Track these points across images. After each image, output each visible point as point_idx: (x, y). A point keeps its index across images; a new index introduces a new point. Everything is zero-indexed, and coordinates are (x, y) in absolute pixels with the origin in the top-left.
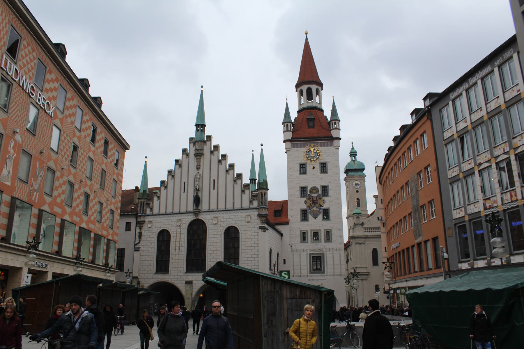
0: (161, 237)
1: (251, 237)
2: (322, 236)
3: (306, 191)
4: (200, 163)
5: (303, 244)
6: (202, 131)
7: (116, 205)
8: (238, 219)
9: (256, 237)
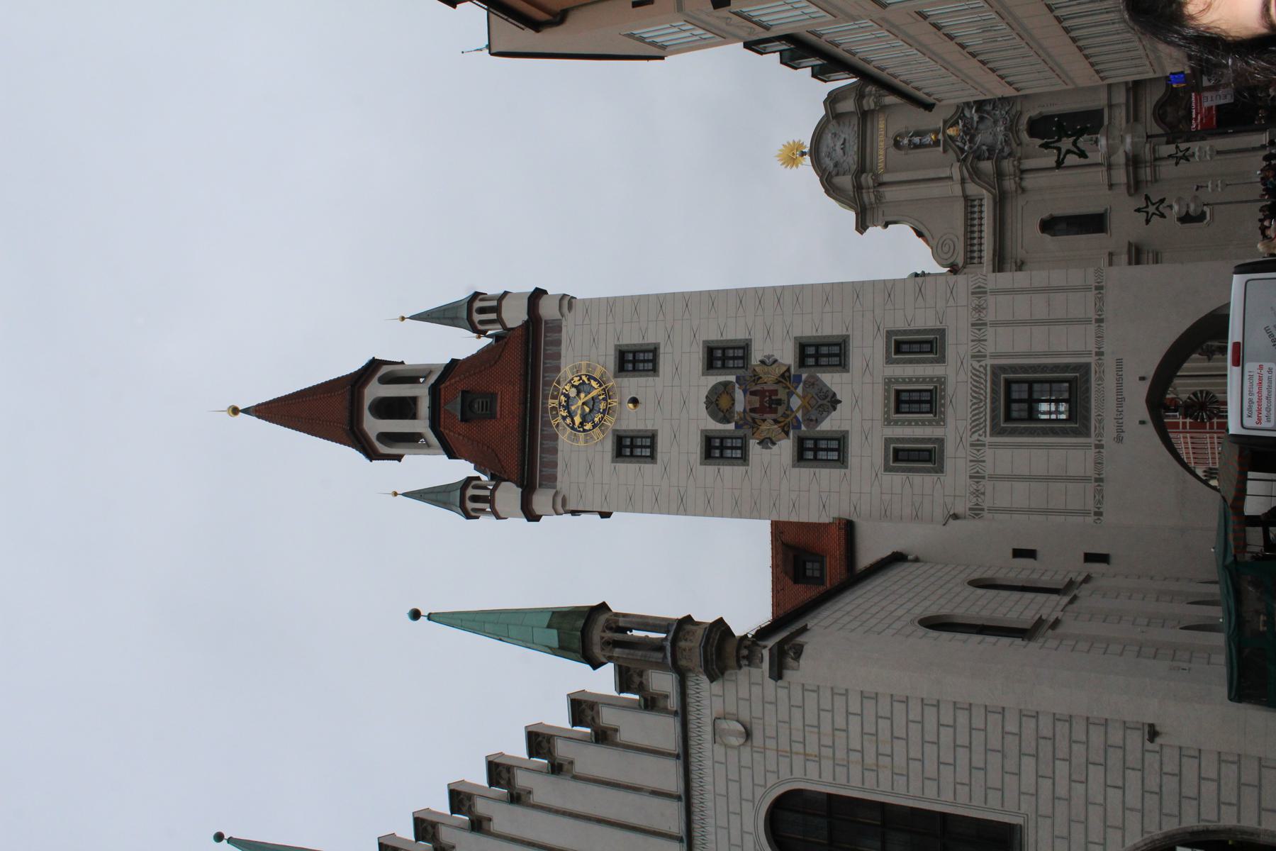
1: (826, 728)
2: (915, 371)
3: (722, 439)
5: (949, 464)
9: (826, 704)
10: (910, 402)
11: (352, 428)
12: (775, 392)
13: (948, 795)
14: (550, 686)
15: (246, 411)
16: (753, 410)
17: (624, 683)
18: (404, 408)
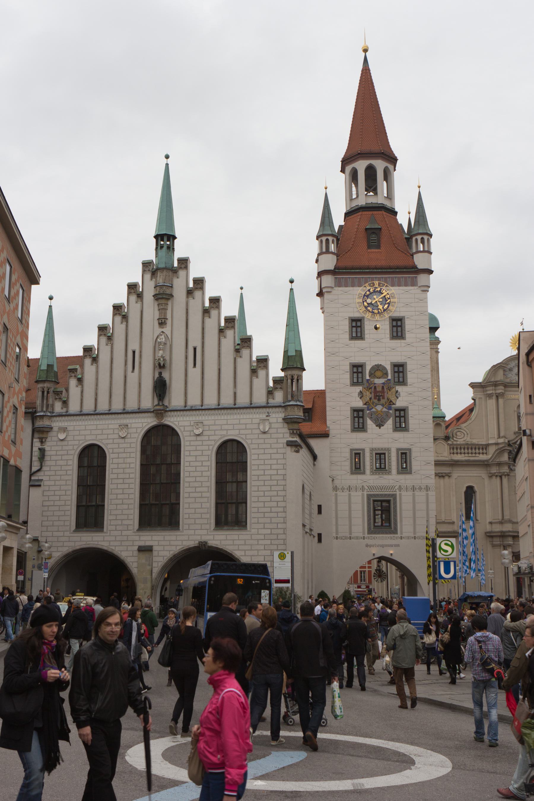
0: (86, 460)
2: (393, 461)
3: (362, 372)
4: (165, 314)
5: (355, 477)
6: (168, 247)
7: (20, 396)
8: (243, 427)
10: (380, 459)
11: (359, 154)
12: (384, 398)
16: (375, 388)
17: (277, 381)
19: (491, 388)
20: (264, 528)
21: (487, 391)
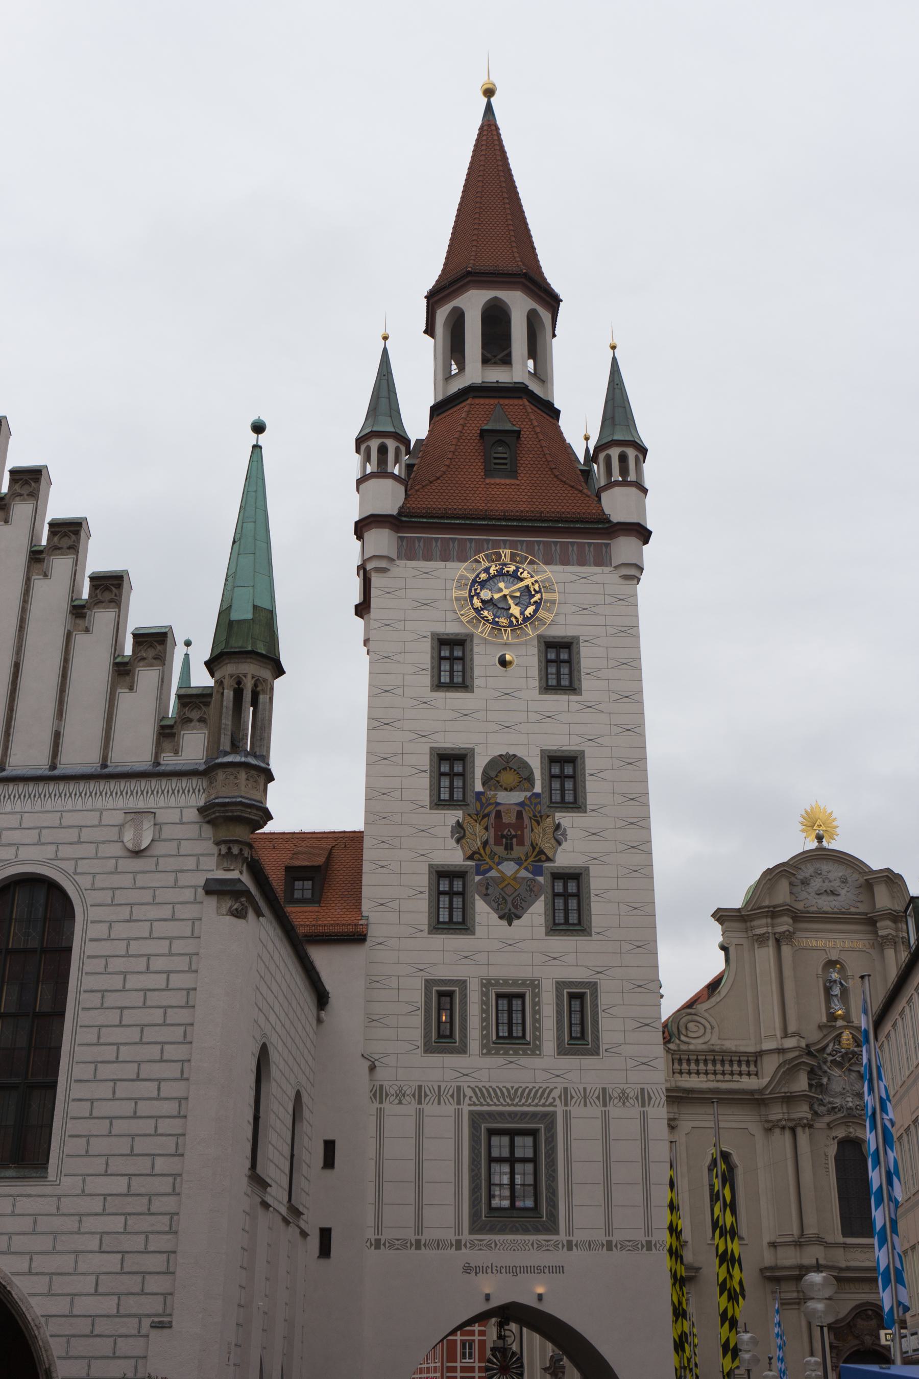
5: (436, 1059)
8: (72, 835)
11: (469, 273)
12: (521, 843)
13: (78, 1091)
14: (182, 603)
15: (489, 109)
16: (499, 815)
17: (192, 700)
18: (496, 346)
19: (764, 921)
20: (106, 1174)
21: (752, 928)
